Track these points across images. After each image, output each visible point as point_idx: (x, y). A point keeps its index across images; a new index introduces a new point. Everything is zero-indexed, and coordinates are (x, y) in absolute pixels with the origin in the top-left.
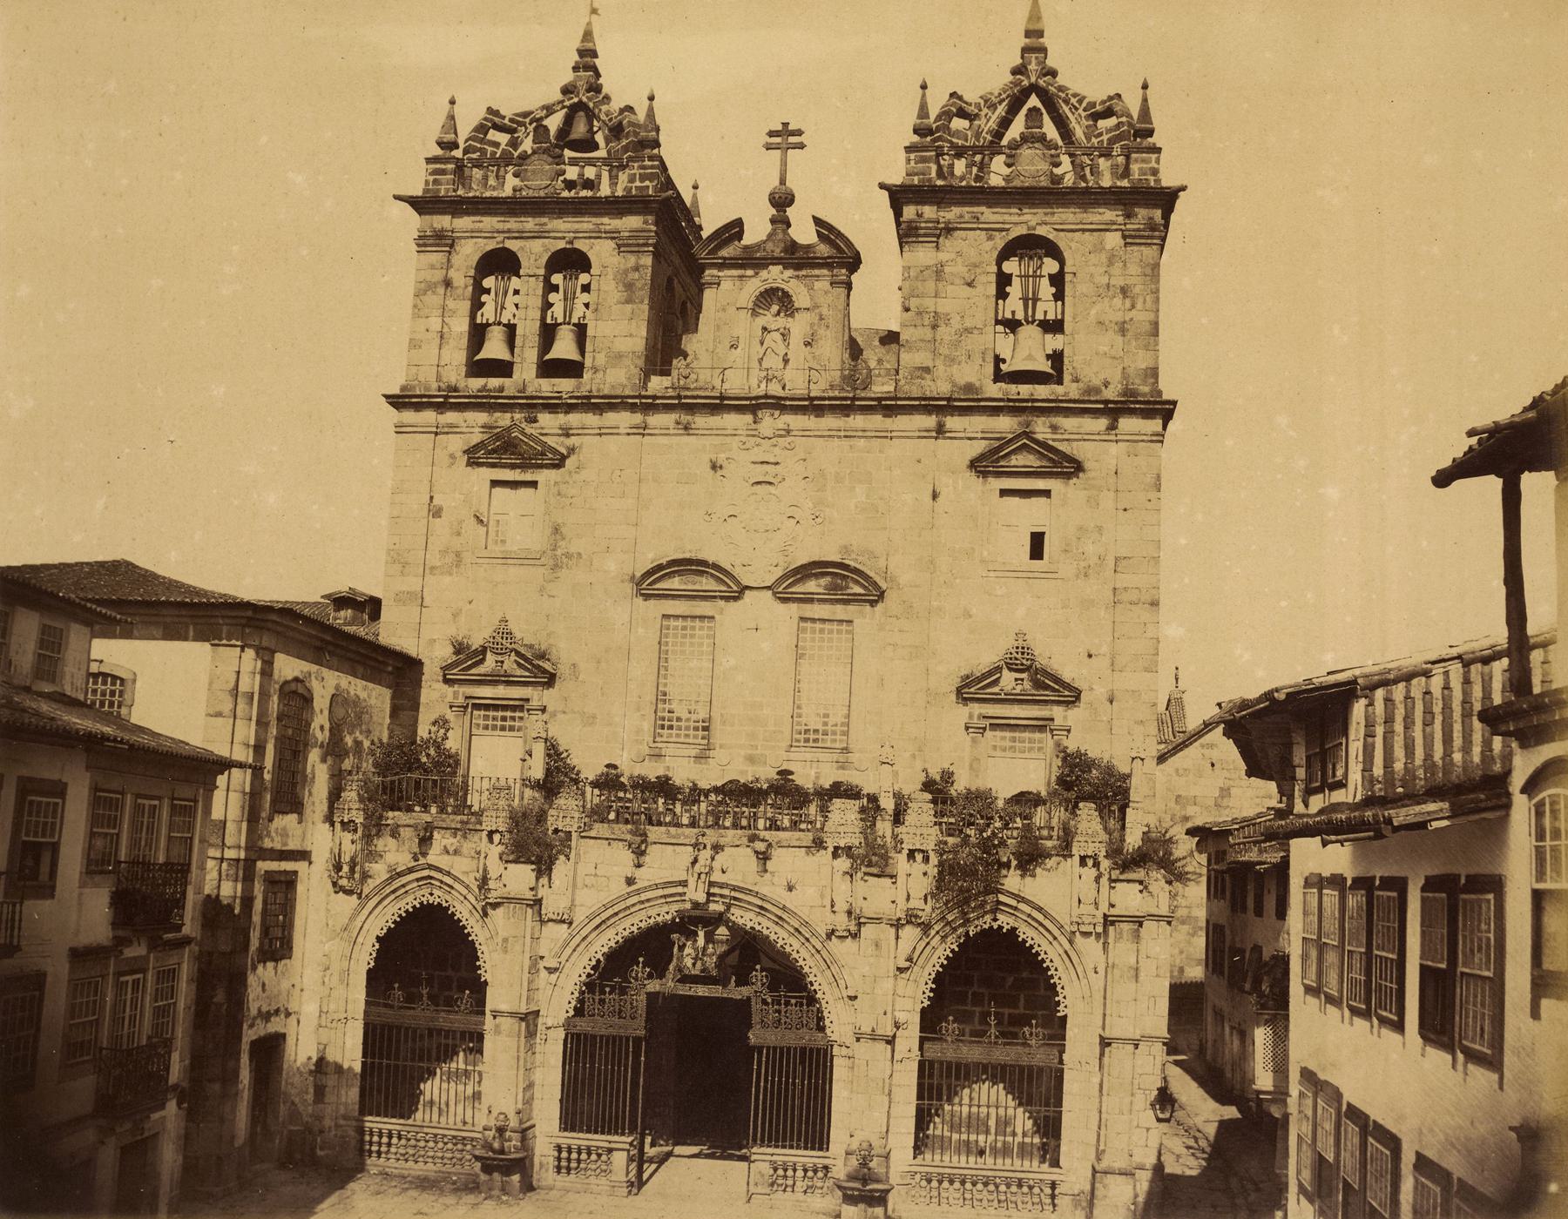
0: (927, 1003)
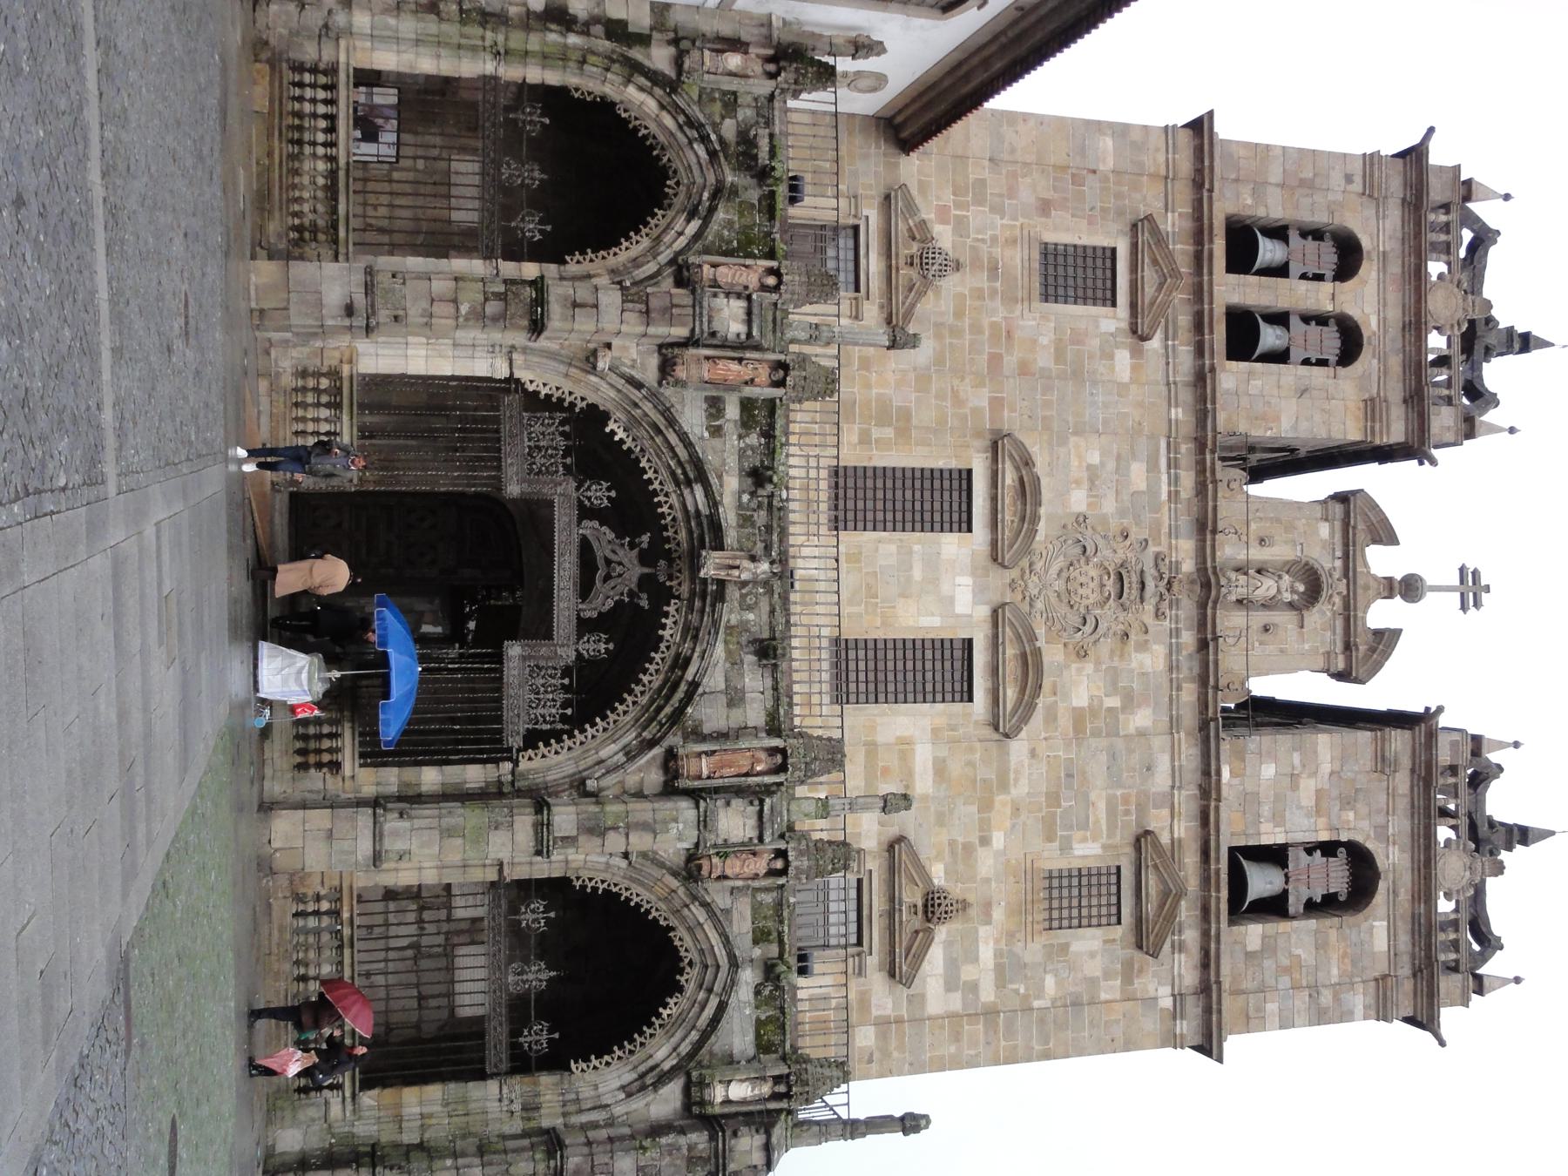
0: (578, 884)
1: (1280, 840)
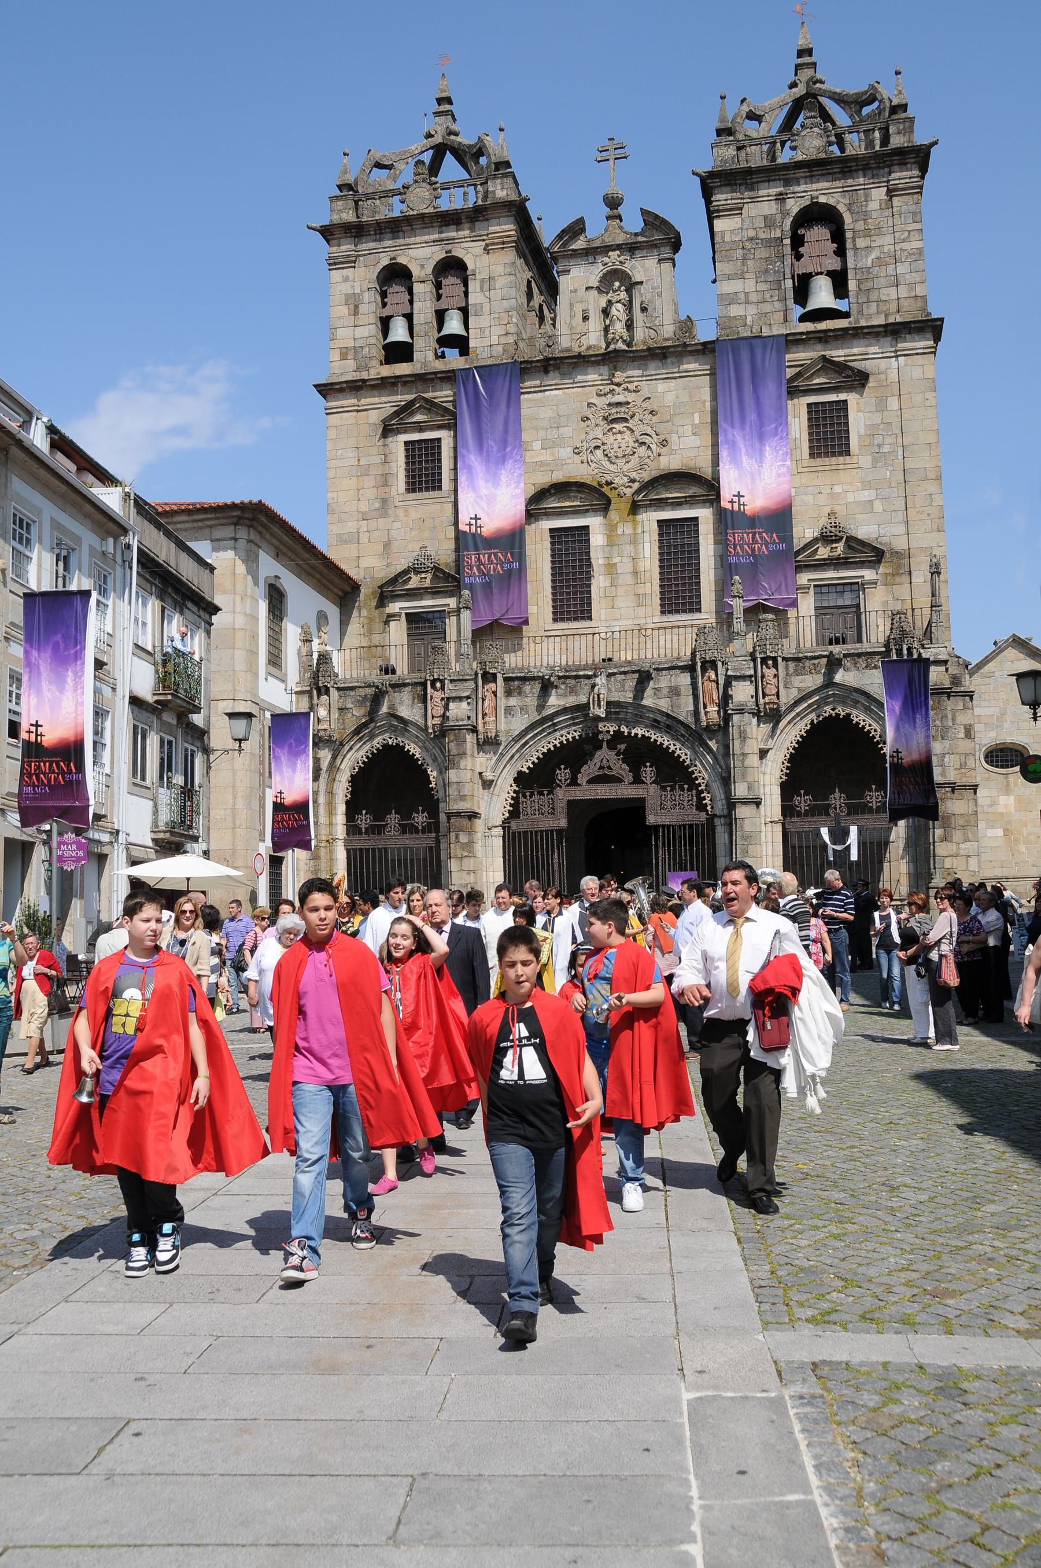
0: (784, 778)
1: (789, 283)
